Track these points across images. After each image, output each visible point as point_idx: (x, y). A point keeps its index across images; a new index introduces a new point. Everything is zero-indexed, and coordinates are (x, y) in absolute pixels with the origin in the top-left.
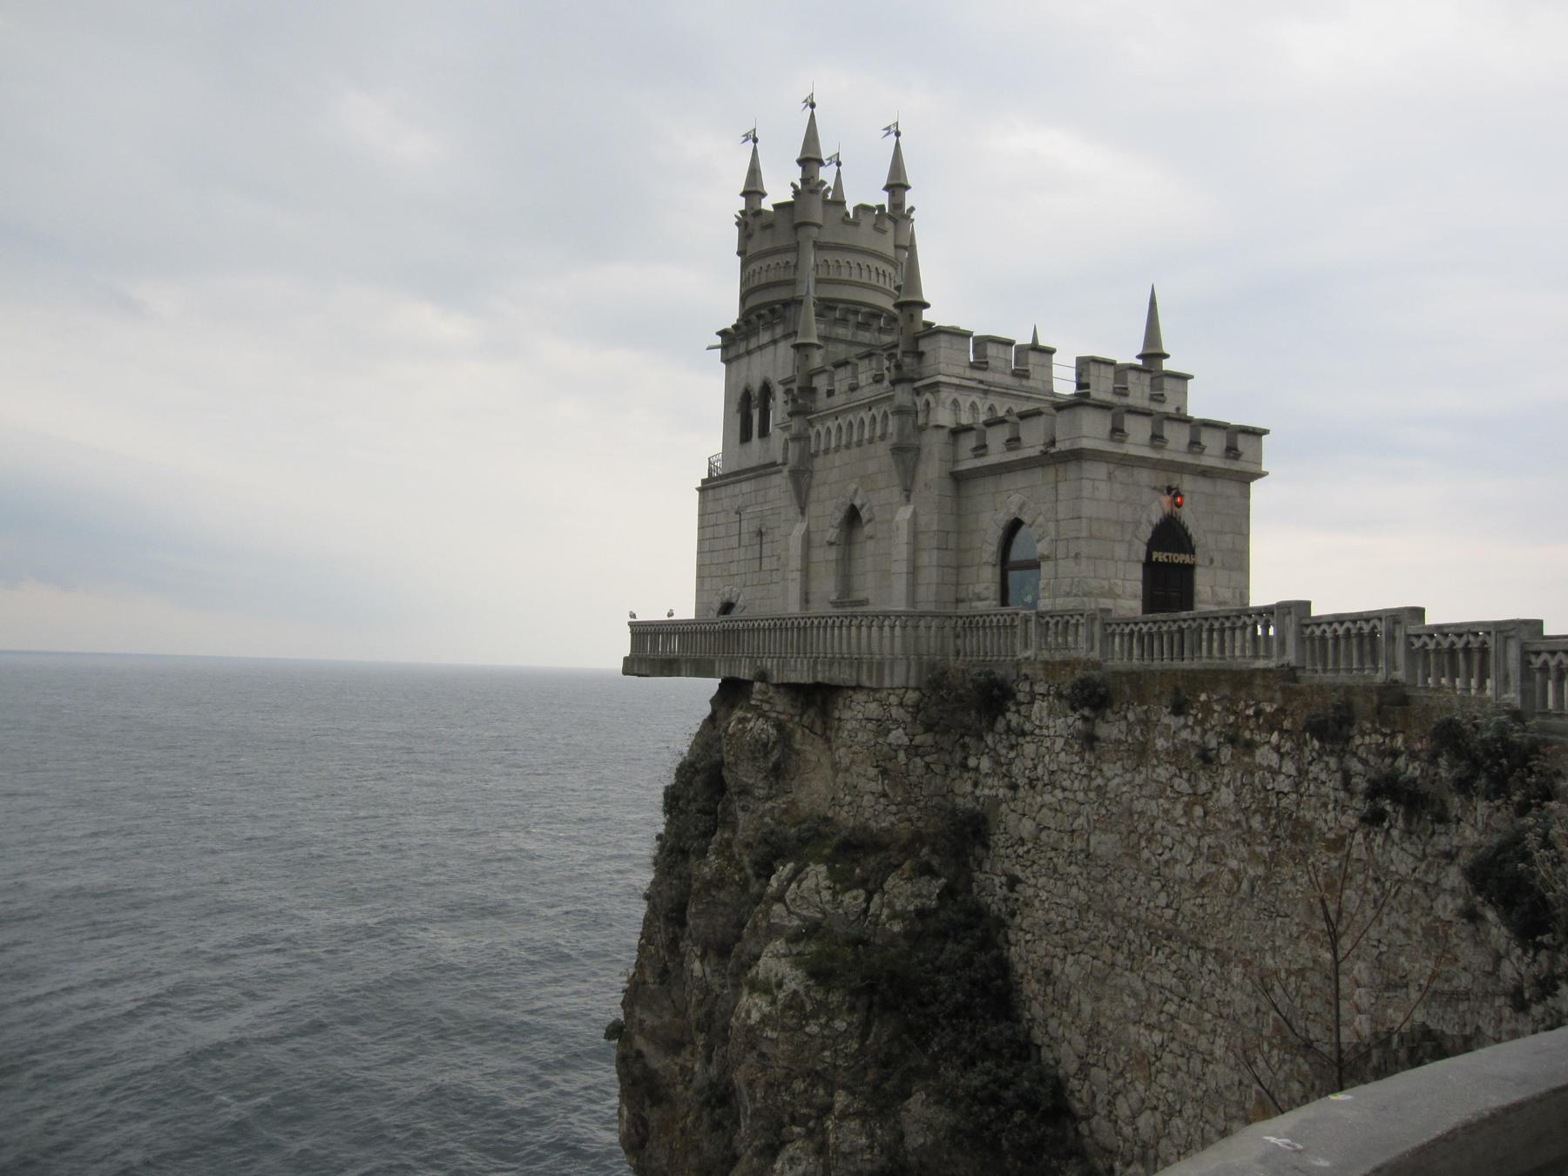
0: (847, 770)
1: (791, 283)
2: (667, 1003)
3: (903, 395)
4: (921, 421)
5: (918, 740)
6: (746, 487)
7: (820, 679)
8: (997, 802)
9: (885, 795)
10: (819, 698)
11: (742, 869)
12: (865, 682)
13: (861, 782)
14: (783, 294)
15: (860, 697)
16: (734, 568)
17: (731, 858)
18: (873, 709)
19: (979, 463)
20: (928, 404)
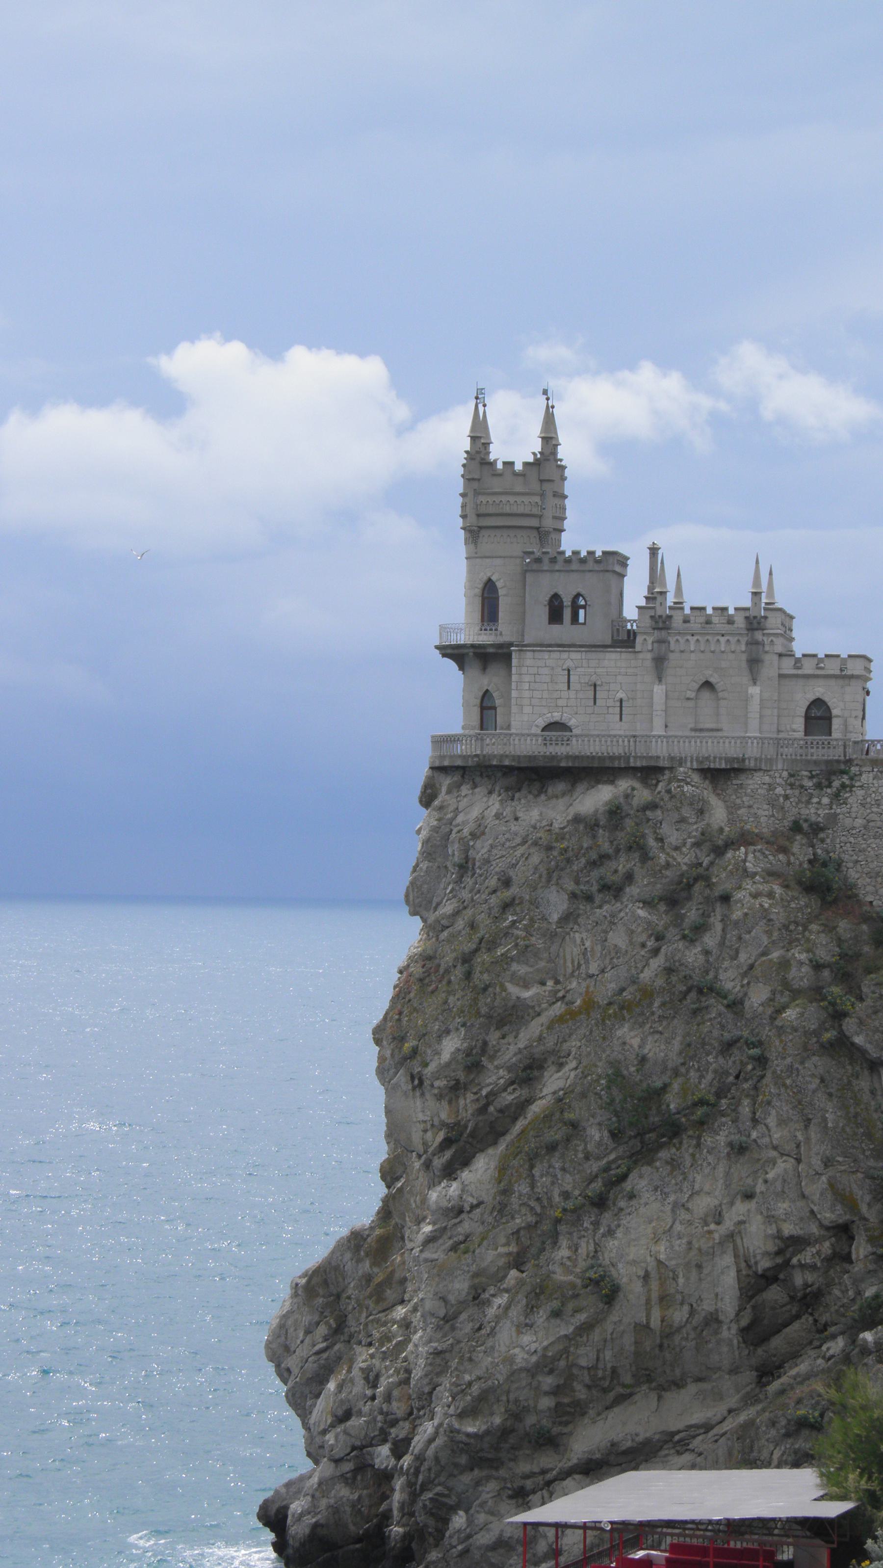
0: (750, 807)
1: (540, 517)
2: (546, 955)
3: (758, 636)
4: (767, 648)
5: (788, 792)
6: (575, 656)
7: (736, 766)
8: (836, 815)
9: (773, 816)
10: (709, 775)
11: (675, 859)
12: (763, 767)
13: (760, 812)
14: (534, 523)
15: (760, 774)
16: (561, 703)
17: (668, 854)
18: (767, 779)
19: (800, 672)
20: (772, 641)
